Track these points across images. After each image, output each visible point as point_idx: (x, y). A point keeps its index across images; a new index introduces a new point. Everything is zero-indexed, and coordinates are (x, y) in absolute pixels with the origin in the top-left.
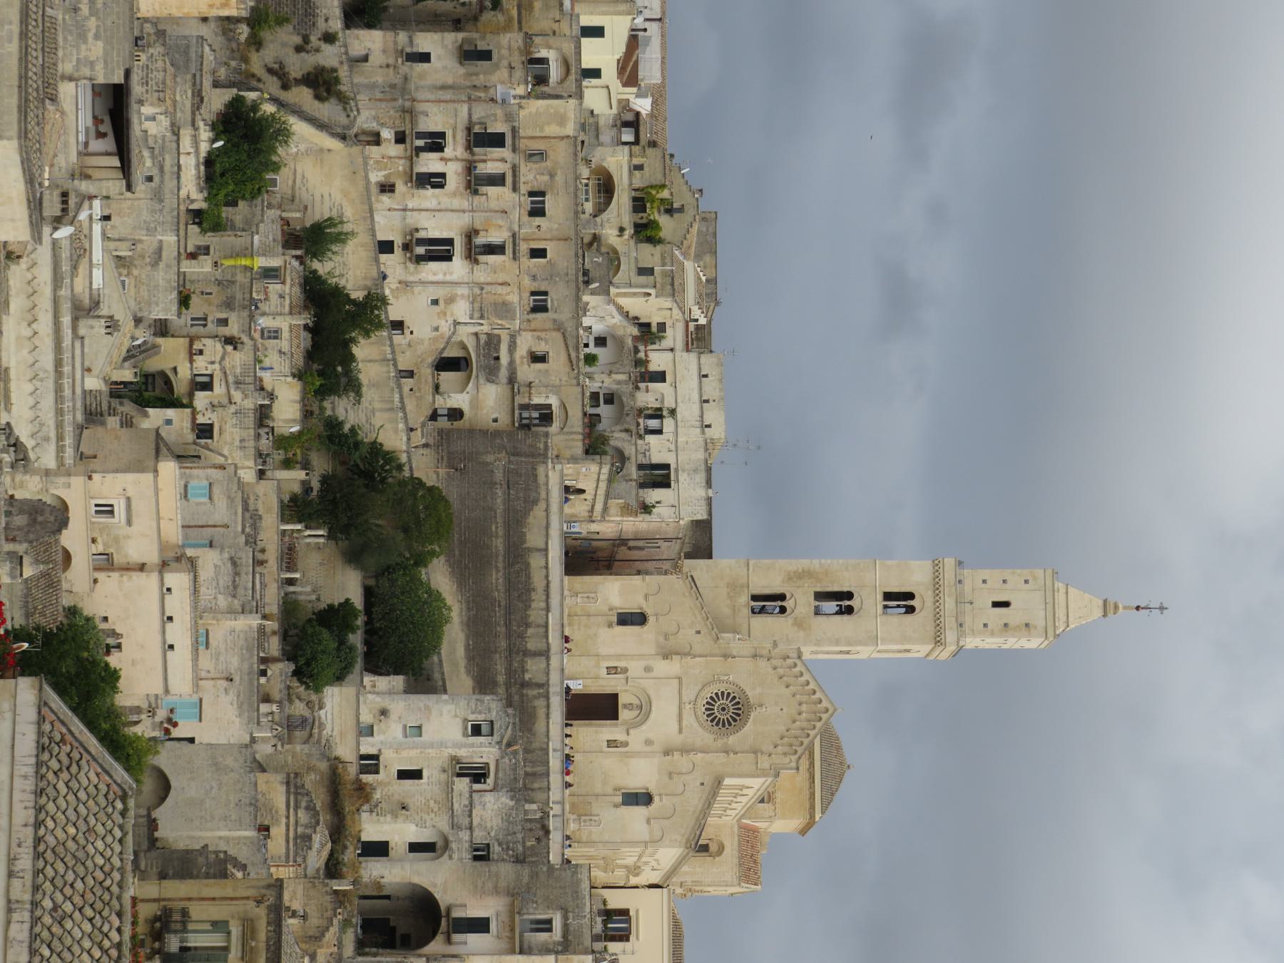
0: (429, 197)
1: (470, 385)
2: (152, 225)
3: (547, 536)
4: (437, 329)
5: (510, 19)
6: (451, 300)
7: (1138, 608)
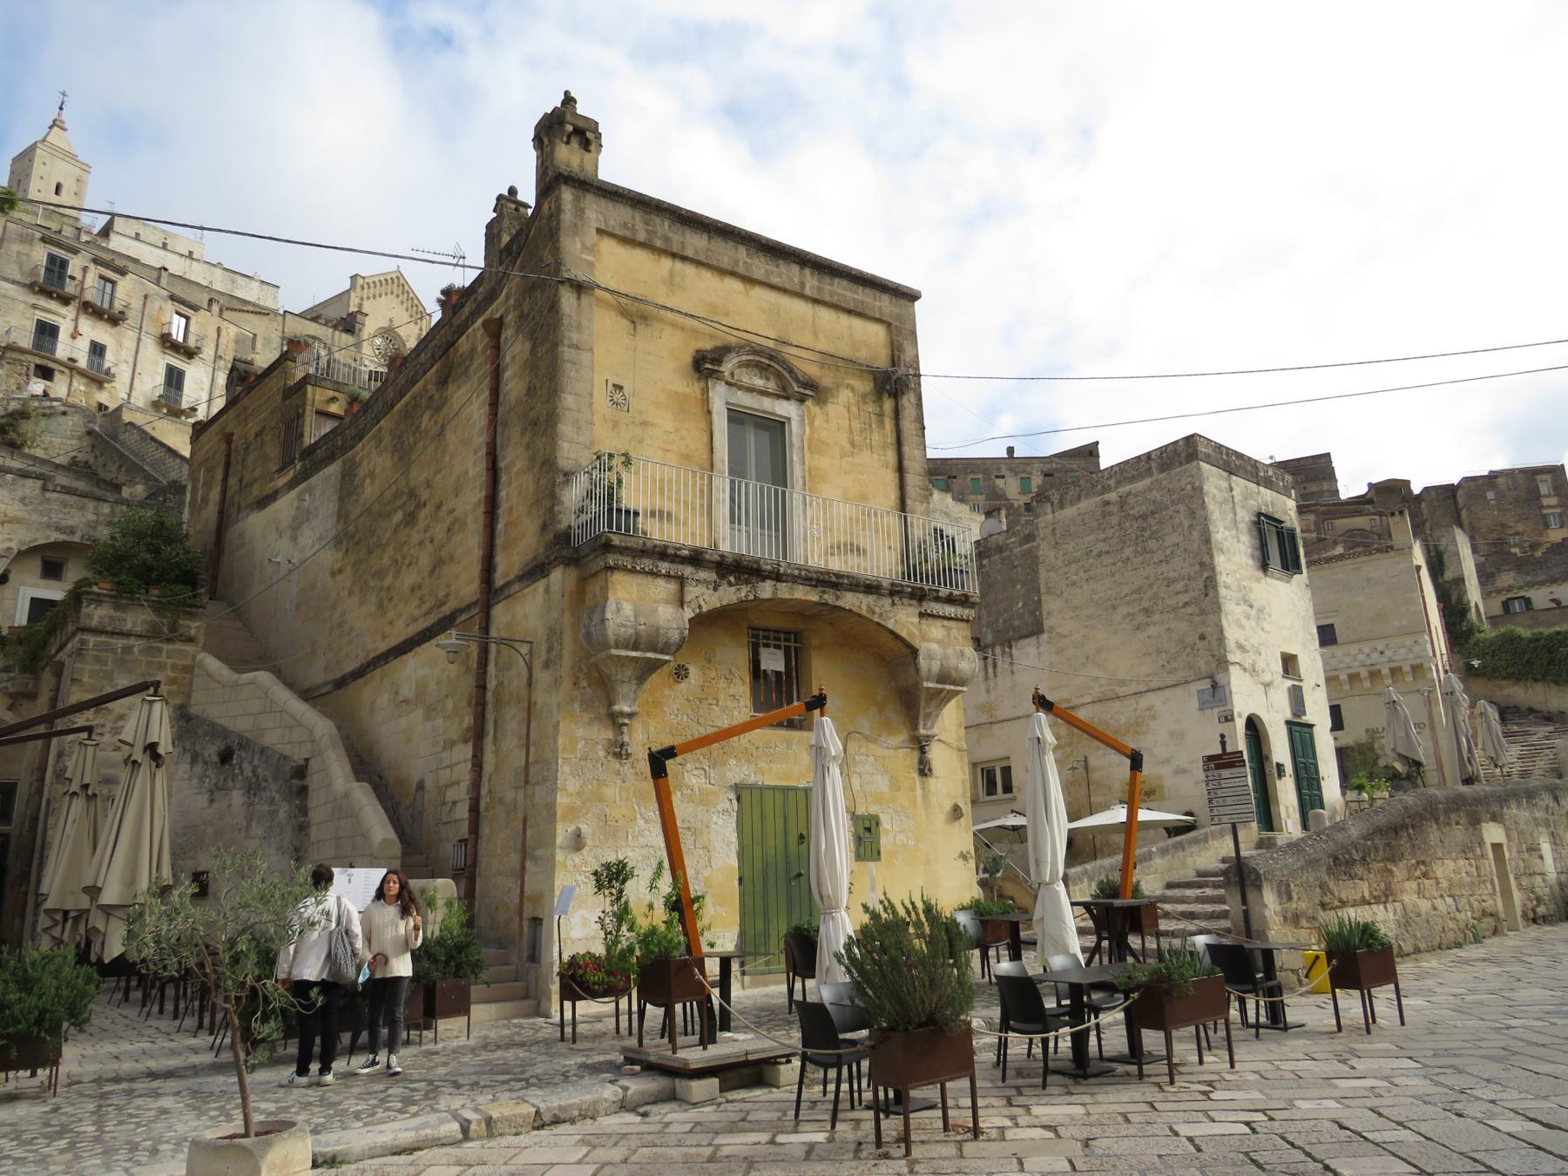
7: (61, 108)
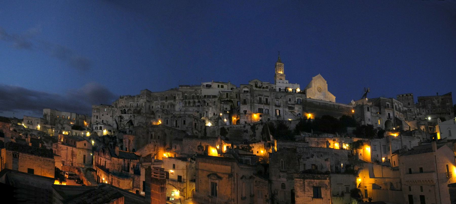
0: (270, 112)
1: (295, 111)
2: (332, 155)
3: (318, 102)
4: (290, 115)
5: (233, 100)
6: (286, 111)
